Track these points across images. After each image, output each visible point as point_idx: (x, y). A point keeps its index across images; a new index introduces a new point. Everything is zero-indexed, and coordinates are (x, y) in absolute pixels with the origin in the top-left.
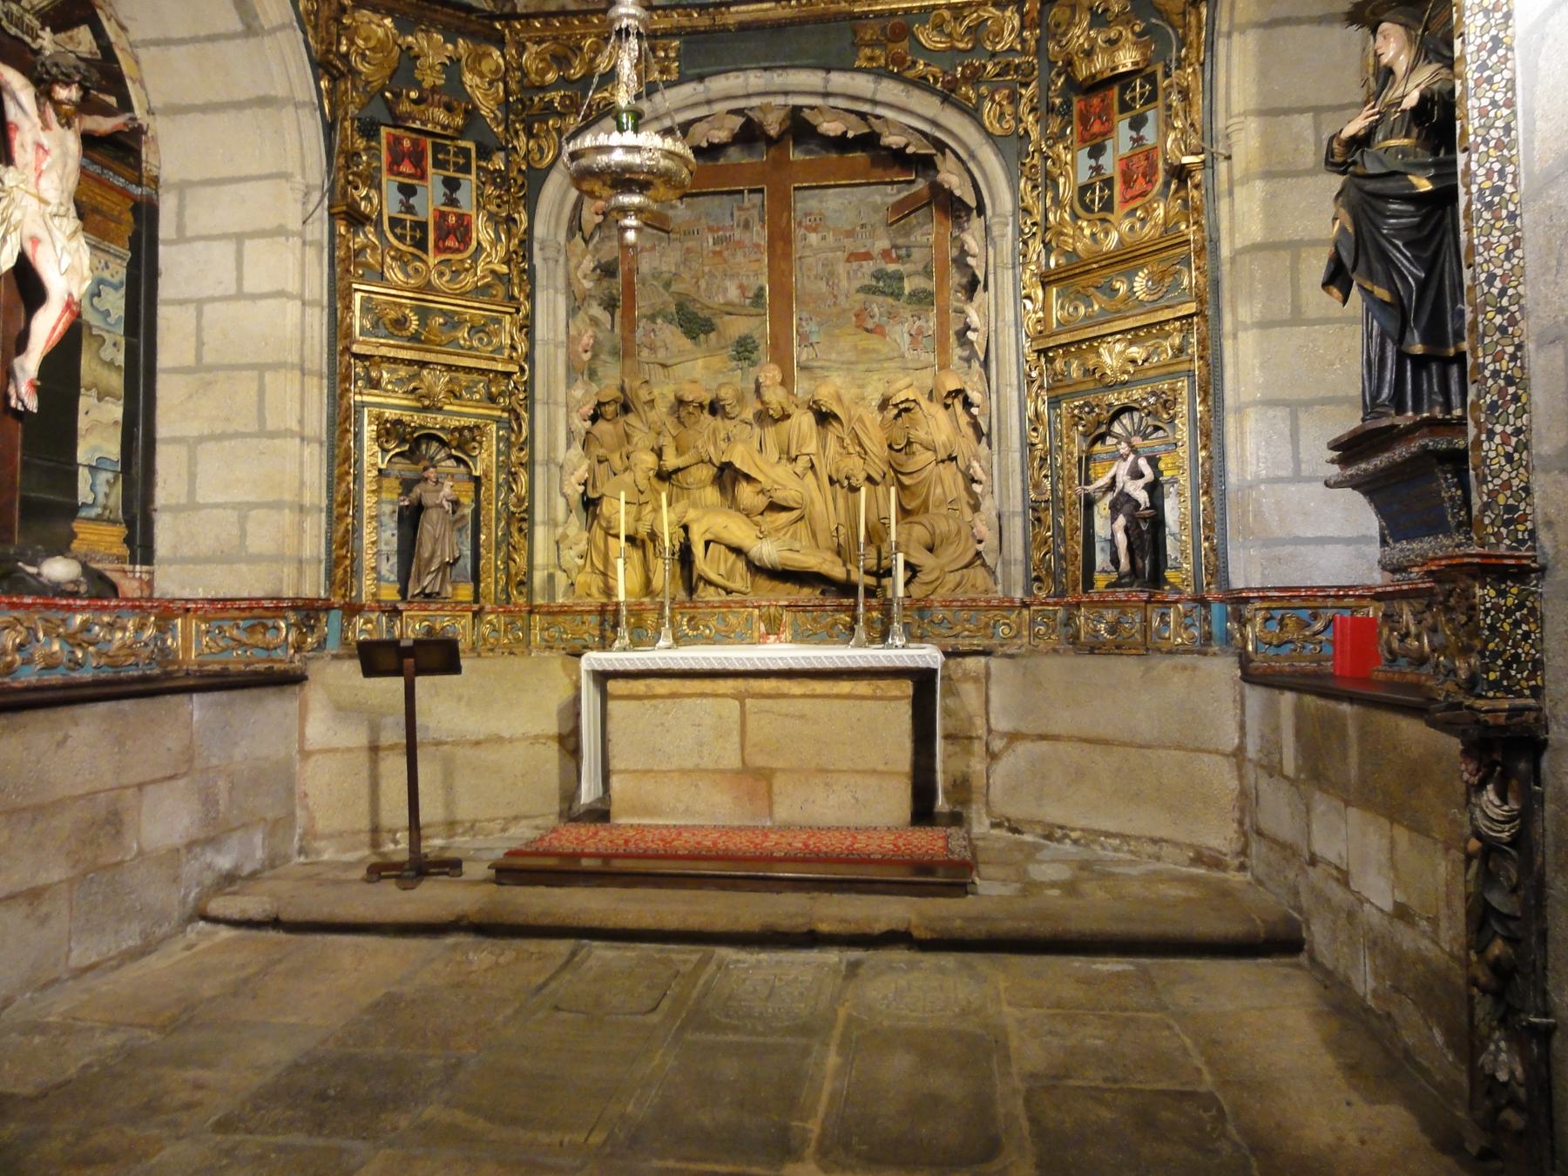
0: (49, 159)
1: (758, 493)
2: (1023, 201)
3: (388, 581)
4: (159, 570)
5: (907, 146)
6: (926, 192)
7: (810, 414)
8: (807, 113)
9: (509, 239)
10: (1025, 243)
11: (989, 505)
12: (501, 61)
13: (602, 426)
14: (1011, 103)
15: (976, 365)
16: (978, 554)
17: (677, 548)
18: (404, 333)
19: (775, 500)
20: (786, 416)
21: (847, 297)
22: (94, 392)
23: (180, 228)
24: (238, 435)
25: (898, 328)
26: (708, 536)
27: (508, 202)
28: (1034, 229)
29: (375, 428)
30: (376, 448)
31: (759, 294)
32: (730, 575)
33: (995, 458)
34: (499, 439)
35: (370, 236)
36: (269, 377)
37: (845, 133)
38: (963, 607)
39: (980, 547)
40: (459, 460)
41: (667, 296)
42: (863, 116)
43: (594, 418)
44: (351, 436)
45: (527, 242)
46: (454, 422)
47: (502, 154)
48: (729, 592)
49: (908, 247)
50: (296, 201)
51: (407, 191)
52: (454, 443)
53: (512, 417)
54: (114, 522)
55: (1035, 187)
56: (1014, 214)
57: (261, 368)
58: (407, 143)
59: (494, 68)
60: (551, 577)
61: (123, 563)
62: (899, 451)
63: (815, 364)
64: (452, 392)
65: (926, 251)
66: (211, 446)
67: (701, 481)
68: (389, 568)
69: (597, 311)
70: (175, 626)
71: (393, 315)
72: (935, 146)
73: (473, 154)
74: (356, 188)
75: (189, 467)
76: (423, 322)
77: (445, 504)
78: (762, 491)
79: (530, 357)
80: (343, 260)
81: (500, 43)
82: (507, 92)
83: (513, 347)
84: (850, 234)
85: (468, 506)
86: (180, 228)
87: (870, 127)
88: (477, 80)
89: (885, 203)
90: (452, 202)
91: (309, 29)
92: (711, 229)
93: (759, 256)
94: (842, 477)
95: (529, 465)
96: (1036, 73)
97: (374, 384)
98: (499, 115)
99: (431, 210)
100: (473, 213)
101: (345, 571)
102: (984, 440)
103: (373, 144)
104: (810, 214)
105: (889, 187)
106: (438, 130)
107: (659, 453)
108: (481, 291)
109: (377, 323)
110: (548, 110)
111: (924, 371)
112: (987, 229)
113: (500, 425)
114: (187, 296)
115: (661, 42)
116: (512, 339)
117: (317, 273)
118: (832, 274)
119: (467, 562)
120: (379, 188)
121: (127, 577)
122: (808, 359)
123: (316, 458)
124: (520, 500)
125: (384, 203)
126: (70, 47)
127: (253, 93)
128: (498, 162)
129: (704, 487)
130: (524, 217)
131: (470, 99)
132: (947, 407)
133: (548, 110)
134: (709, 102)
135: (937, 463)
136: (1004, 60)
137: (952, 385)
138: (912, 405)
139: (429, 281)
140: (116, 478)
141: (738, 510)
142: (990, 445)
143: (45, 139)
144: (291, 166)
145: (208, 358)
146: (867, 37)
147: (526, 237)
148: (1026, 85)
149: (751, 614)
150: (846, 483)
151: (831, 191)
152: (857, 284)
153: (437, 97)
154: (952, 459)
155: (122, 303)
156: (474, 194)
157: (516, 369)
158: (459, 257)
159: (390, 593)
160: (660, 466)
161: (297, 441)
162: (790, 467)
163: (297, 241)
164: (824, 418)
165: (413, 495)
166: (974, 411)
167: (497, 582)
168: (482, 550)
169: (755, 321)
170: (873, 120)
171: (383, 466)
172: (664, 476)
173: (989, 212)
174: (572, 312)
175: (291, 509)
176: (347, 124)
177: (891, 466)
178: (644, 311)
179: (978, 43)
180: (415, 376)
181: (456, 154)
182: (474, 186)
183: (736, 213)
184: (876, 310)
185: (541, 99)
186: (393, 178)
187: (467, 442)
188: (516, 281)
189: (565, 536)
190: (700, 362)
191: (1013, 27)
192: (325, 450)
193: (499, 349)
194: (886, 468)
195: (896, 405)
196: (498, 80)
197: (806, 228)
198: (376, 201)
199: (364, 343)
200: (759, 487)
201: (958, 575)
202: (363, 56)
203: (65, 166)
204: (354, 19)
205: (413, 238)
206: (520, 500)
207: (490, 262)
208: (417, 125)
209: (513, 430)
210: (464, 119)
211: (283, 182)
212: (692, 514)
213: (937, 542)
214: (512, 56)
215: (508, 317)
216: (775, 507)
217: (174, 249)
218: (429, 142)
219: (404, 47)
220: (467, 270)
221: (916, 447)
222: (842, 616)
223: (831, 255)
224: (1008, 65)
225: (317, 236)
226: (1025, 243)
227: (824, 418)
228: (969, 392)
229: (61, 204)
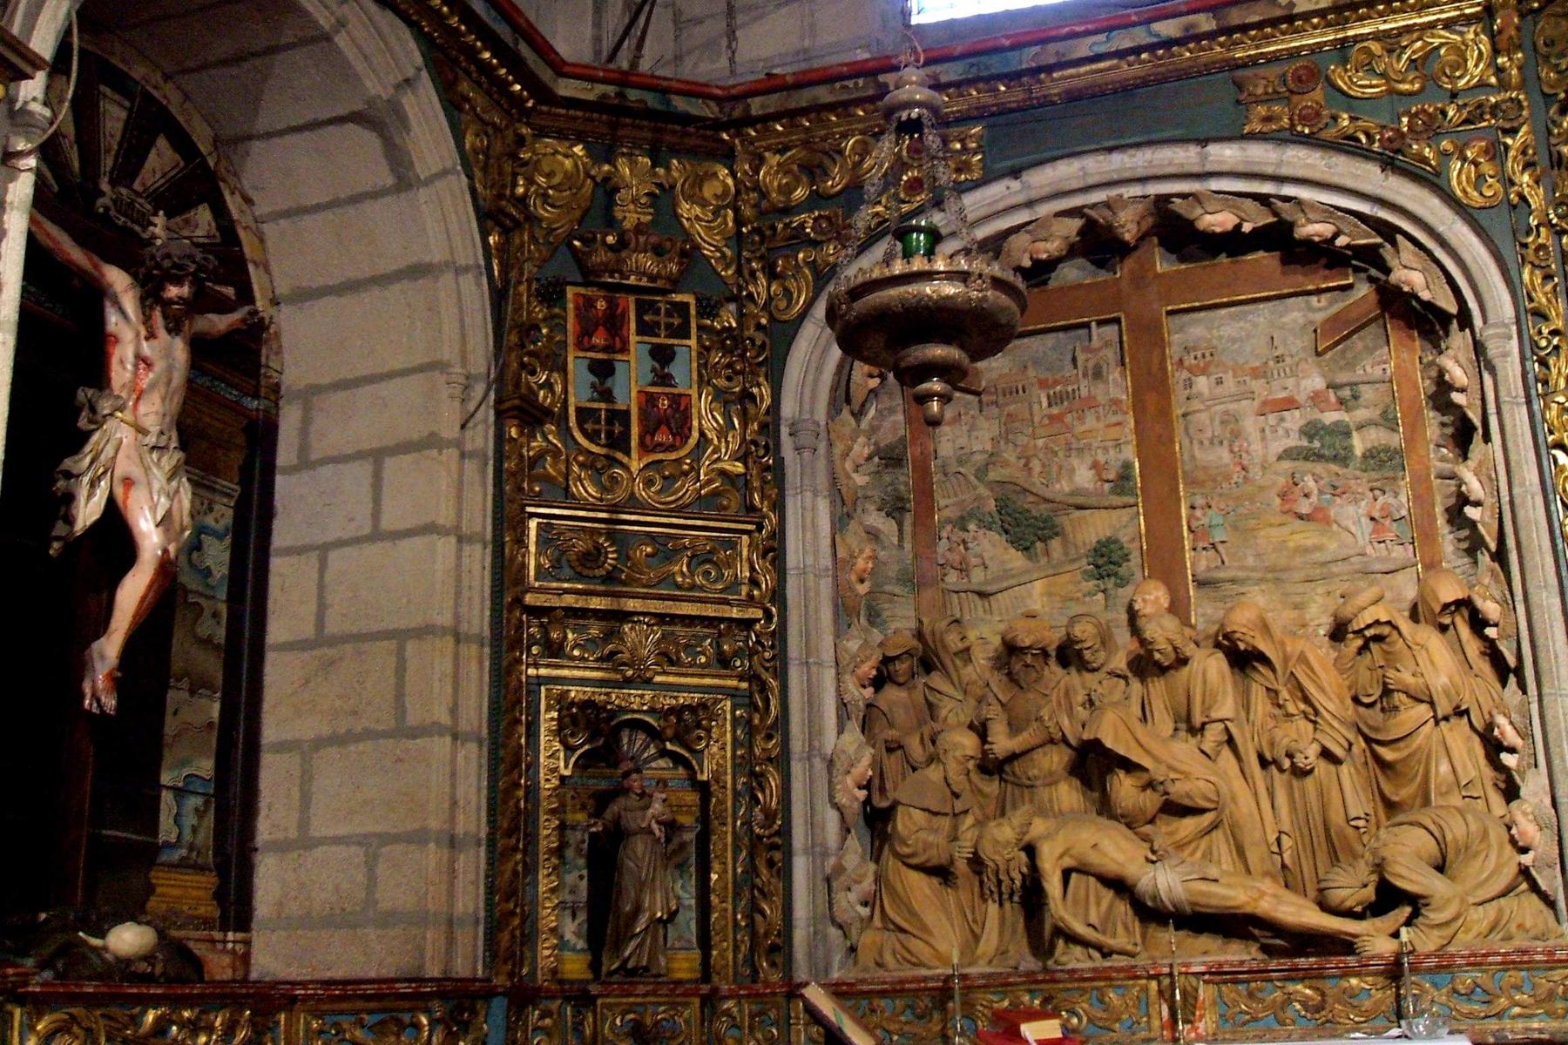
0: (151, 375)
1: (1144, 788)
2: (1531, 300)
3: (574, 949)
4: (259, 939)
5: (1336, 235)
6: (1373, 298)
7: (1220, 655)
8: (1178, 205)
9: (744, 425)
10: (1543, 363)
12: (730, 181)
13: (892, 694)
14: (1492, 159)
15: (1484, 559)
16: (1524, 872)
17: (1018, 883)
18: (597, 572)
19: (1171, 797)
20: (1182, 661)
21: (1264, 468)
22: (185, 684)
23: (304, 449)
24: (368, 734)
25: (1351, 509)
26: (1068, 862)
27: (742, 372)
28: (1555, 341)
29: (555, 715)
30: (557, 746)
31: (1125, 475)
32: (1105, 925)
34: (735, 720)
35: (551, 437)
36: (411, 647)
37: (1238, 227)
38: (1507, 965)
39: (1527, 859)
40: (677, 759)
41: (983, 491)
42: (1263, 199)
43: (878, 682)
44: (523, 729)
45: (770, 426)
46: (668, 702)
47: (732, 307)
48: (1106, 953)
49: (1352, 385)
50: (452, 397)
51: (603, 370)
52: (670, 732)
53: (755, 688)
54: (201, 869)
55: (1548, 277)
56: (1518, 322)
57: (400, 636)
58: (601, 305)
59: (719, 191)
61: (212, 929)
62: (1370, 706)
63: (1221, 575)
64: (664, 654)
65: (1383, 387)
66: (333, 752)
67: (1051, 774)
68: (571, 929)
69: (876, 519)
70: (278, 1023)
71: (581, 545)
72: (1380, 234)
73: (693, 312)
74: (533, 373)
75: (302, 784)
76: (624, 556)
77: (655, 826)
78: (1150, 785)
79: (778, 595)
80: (514, 474)
81: (728, 157)
82: (739, 222)
83: (754, 582)
84: (1256, 373)
85: (690, 829)
86: (304, 449)
87: (1275, 214)
88: (697, 210)
89: (1311, 322)
90: (664, 379)
91: (478, 174)
92: (1043, 384)
93: (1119, 418)
94: (1280, 753)
95: (782, 761)
96: (1525, 113)
97: (554, 650)
98: (728, 252)
99: (634, 394)
100: (694, 392)
101: (513, 936)
102: (1512, 679)
103: (557, 310)
104: (1195, 349)
105: (1314, 299)
106: (644, 282)
107: (981, 730)
108: (707, 503)
109: (558, 560)
110: (798, 239)
111: (1400, 576)
112: (1479, 348)
113: (738, 700)
114: (307, 541)
115: (954, 131)
117: (479, 498)
118: (1236, 434)
120: (563, 370)
121: (214, 950)
122: (1209, 569)
123: (474, 764)
124: (770, 816)
125: (571, 389)
126: (186, 233)
127: (401, 264)
128: (728, 318)
129: (1056, 783)
130: (766, 391)
131: (687, 236)
132: (1443, 629)
133: (798, 239)
134: (1030, 204)
135: (1437, 723)
136: (1472, 100)
137: (1449, 592)
138: (1386, 630)
139: (633, 493)
140: (207, 803)
141: (1113, 817)
142: (1524, 690)
143: (146, 348)
144: (449, 353)
145: (333, 627)
146: (1260, 91)
147: (769, 419)
148: (1513, 132)
149: (1146, 989)
150: (1287, 764)
151: (1223, 312)
152: (1277, 447)
153: (642, 239)
154: (1461, 713)
155: (226, 556)
156: (695, 365)
157: (759, 614)
158: (673, 456)
159: (575, 966)
160: (984, 753)
161: (448, 739)
162: (1193, 741)
163: (453, 453)
164: (1243, 659)
165: (608, 815)
166: (1491, 632)
167: (736, 949)
168: (714, 899)
169: (1125, 515)
170: (1279, 204)
171: (567, 773)
172: (991, 766)
173: (1478, 322)
174: (840, 522)
175: (438, 842)
176: (523, 288)
177: (1360, 731)
178: (947, 513)
179: (1430, 81)
180: (609, 635)
181: (669, 314)
182: (694, 354)
183: (1081, 358)
184: (1311, 484)
185: (787, 226)
186: (581, 354)
187: (688, 730)
188: (756, 484)
189: (840, 869)
190: (1038, 584)
191: (1480, 53)
192: (485, 749)
193: (734, 585)
194: (1351, 736)
195: (1359, 632)
196: (727, 206)
197: (1190, 370)
198: (558, 388)
199: (541, 590)
200: (1145, 777)
201: (1492, 909)
202: (545, 196)
203: (169, 381)
204: (534, 153)
205: (609, 434)
206: (770, 816)
207: (719, 459)
208: (616, 279)
209: (756, 708)
210: (680, 264)
211: (437, 374)
212: (1039, 827)
213: (1450, 856)
214: (746, 172)
215: (745, 538)
216: (1176, 809)
217: (294, 479)
218: (632, 299)
219: (599, 180)
220: (686, 474)
221: (1399, 698)
222: (1299, 987)
223: (1232, 406)
224: (1480, 106)
225: (479, 442)
226: (1543, 363)
227: (1243, 659)
228: (1479, 603)
229: (162, 433)
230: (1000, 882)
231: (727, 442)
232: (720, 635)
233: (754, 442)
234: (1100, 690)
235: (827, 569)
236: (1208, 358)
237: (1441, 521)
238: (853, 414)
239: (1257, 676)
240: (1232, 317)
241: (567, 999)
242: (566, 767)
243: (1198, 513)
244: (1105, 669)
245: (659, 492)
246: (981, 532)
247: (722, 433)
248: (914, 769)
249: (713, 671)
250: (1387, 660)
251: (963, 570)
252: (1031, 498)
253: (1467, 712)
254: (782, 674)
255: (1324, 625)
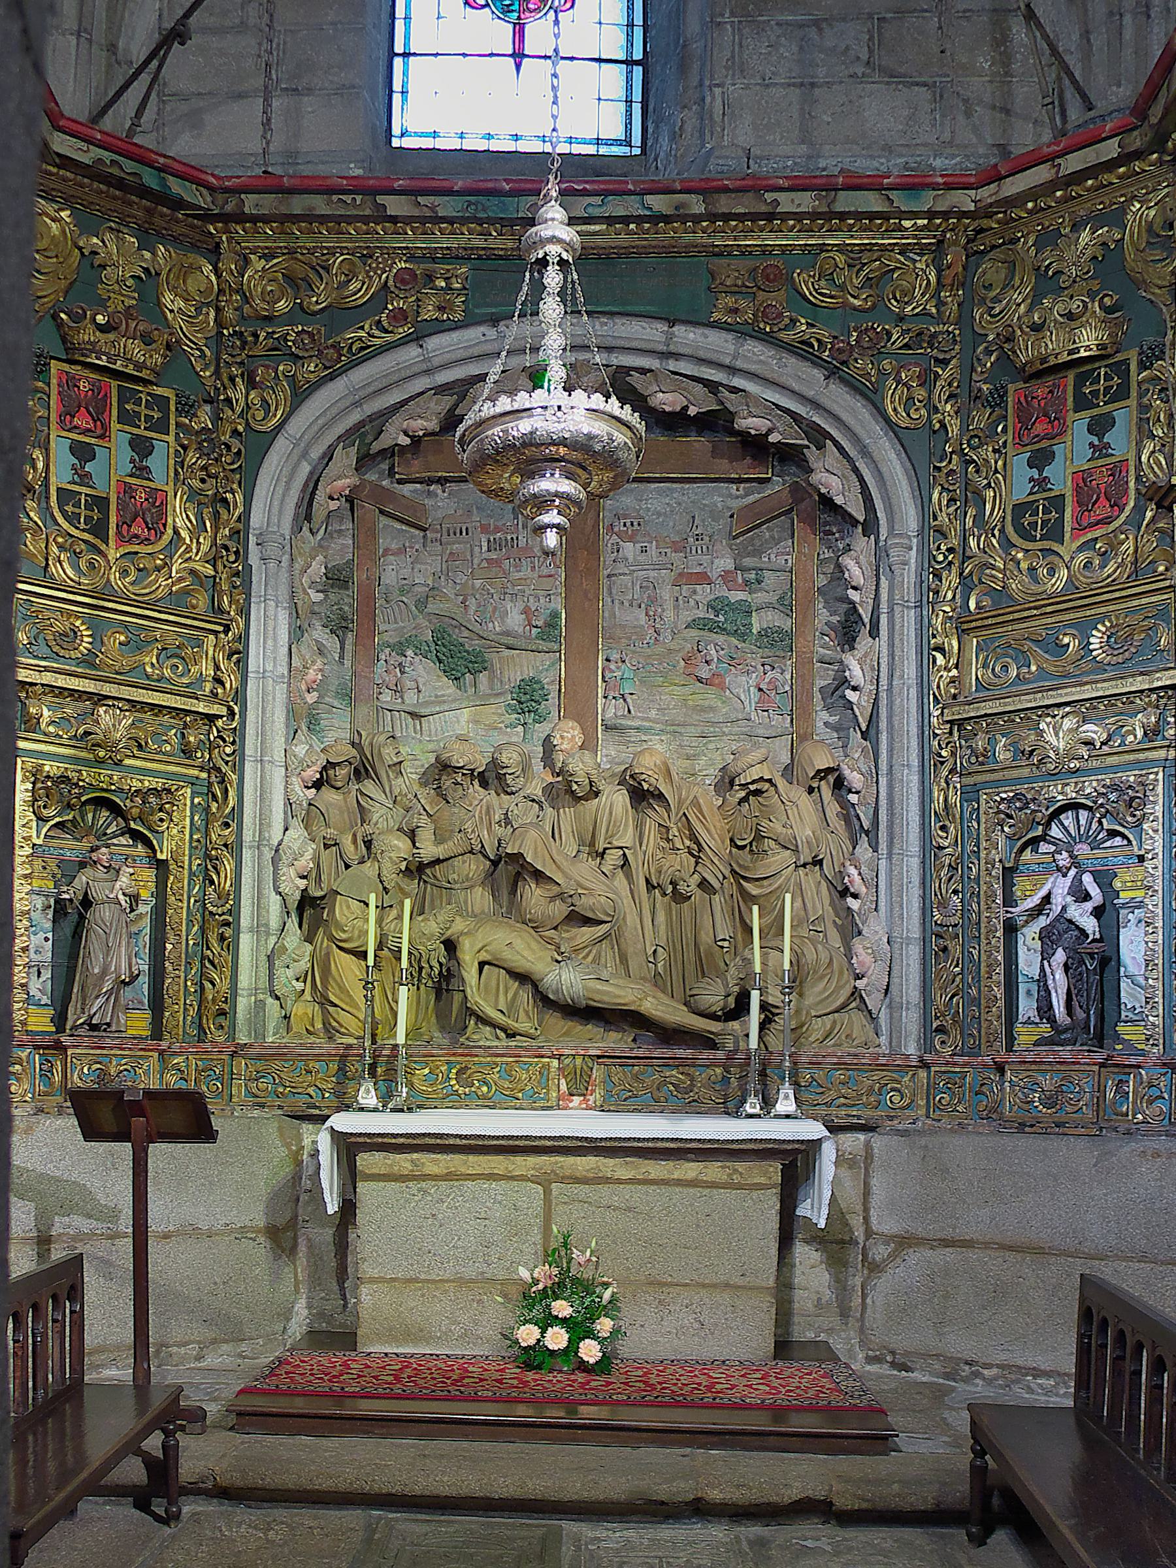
11: (875, 929)
19: (576, 909)
26: (484, 956)
31: (552, 622)
33: (883, 863)
40: (136, 836)
43: (317, 785)
45: (240, 534)
47: (207, 408)
48: (511, 1035)
53: (213, 778)
60: (260, 1005)
65: (784, 576)
77: (121, 897)
79: (240, 695)
83: (219, 681)
90: (142, 471)
92: (485, 529)
93: (552, 570)
94: (665, 880)
95: (235, 848)
104: (626, 516)
107: (412, 835)
108: (178, 601)
110: (279, 350)
113: (197, 788)
116: (217, 667)
118: (653, 600)
119: (144, 983)
124: (223, 896)
128: (204, 417)
130: (239, 498)
132: (811, 790)
147: (241, 526)
151: (653, 486)
152: (687, 616)
156: (172, 462)
157: (224, 711)
158: (149, 549)
169: (548, 659)
174: (297, 633)
177: (733, 871)
180: (82, 717)
184: (713, 652)
215: (211, 637)
223: (652, 574)
228: (846, 772)
230: (421, 968)
231: (198, 543)
232: (186, 726)
233: (226, 548)
234: (516, 812)
235: (283, 676)
236: (636, 527)
237: (818, 696)
238: (311, 530)
239: (650, 812)
240: (660, 492)
241: (36, 1047)
242: (38, 837)
243: (613, 666)
244: (522, 793)
245: (132, 584)
246: (417, 659)
247: (195, 533)
248: (347, 867)
249: (177, 760)
250: (761, 811)
251: (398, 691)
252: (466, 633)
253: (820, 862)
254: (239, 767)
255: (711, 774)
